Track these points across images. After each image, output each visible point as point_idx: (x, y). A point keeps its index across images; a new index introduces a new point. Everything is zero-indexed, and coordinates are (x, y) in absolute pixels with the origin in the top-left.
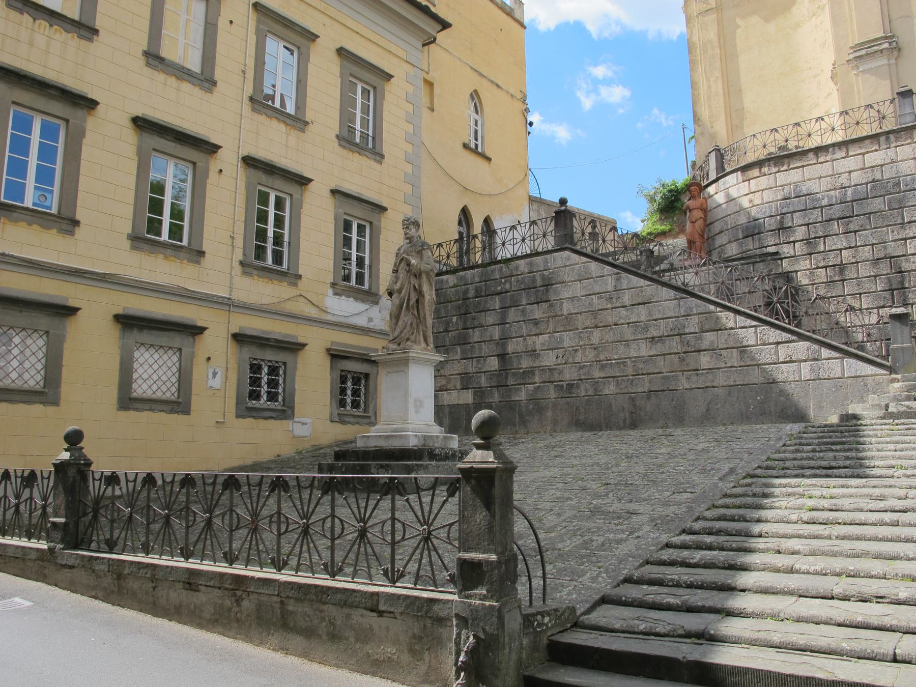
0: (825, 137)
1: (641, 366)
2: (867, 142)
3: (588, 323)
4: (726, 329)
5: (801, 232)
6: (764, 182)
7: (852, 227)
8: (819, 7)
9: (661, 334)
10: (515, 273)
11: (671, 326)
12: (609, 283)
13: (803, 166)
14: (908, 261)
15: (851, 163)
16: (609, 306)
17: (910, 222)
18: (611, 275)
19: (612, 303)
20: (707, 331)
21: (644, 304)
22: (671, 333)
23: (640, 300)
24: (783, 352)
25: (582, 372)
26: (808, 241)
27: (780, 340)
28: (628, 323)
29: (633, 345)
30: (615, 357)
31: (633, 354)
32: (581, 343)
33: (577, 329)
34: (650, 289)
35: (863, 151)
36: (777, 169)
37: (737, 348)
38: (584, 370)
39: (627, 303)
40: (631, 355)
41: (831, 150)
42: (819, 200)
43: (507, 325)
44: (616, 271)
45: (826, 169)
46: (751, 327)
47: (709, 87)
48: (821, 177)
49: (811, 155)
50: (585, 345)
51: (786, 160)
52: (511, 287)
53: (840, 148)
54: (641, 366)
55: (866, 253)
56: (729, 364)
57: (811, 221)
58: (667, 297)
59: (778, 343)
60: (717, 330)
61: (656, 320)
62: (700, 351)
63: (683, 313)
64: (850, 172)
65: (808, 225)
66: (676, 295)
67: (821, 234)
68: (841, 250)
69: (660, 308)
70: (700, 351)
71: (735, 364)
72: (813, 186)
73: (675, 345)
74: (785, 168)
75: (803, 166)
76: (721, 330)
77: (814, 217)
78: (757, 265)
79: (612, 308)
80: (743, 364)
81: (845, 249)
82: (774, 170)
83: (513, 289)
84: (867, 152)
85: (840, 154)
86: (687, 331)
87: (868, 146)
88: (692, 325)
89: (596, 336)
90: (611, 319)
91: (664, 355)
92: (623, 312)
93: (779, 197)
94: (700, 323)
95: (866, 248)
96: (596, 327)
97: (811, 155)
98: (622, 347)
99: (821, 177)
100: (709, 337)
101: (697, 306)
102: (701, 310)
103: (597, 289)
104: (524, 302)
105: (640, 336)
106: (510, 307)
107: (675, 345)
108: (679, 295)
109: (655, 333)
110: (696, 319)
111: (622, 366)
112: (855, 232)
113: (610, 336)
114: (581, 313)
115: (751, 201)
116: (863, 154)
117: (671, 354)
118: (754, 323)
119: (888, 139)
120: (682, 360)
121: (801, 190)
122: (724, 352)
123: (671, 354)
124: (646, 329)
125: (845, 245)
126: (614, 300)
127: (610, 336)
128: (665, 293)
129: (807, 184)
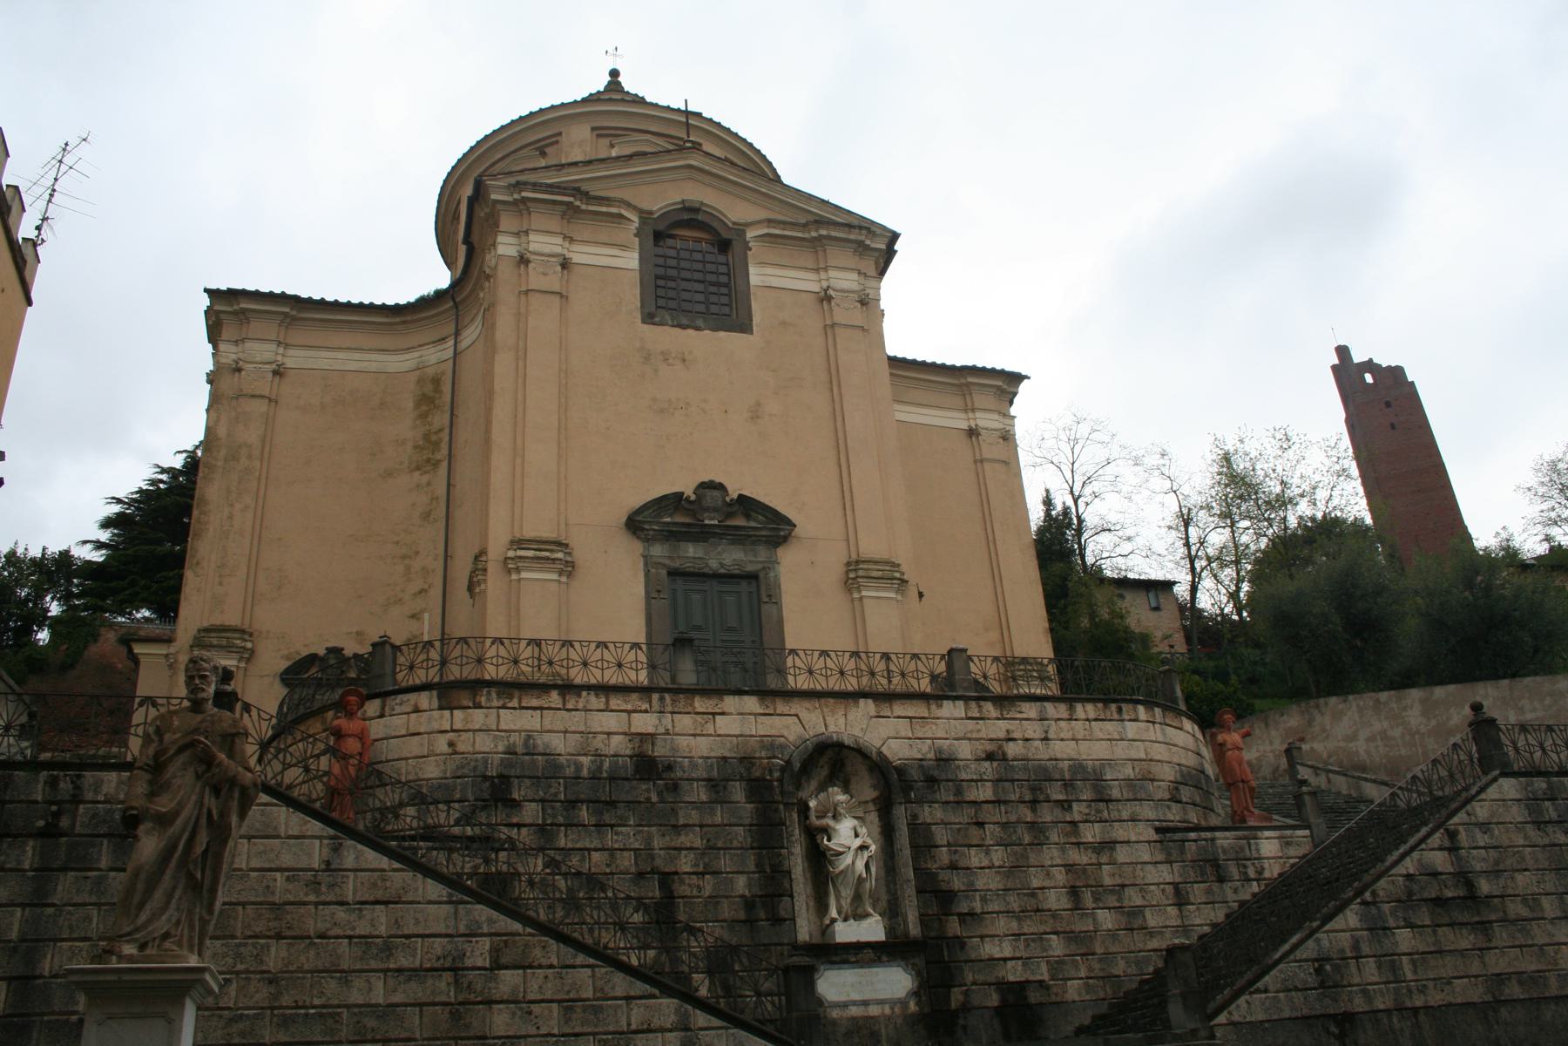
0: (607, 674)
1: (371, 1023)
2: (635, 696)
3: (259, 928)
4: (540, 967)
5: (531, 812)
6: (478, 717)
7: (607, 818)
8: (428, 460)
9: (417, 964)
10: (89, 796)
11: (439, 951)
12: (315, 854)
13: (541, 708)
14: (682, 882)
15: (611, 721)
16: (312, 898)
17: (686, 826)
18: (320, 838)
19: (317, 892)
20: (506, 968)
21: (386, 903)
22: (438, 965)
23: (379, 895)
24: (636, 1015)
25: (235, 1028)
26: (542, 830)
27: (632, 993)
28: (350, 937)
29: (358, 982)
30: (317, 1002)
31: (356, 997)
32: (240, 967)
33: (233, 937)
34: (401, 878)
35: (629, 707)
36: (501, 703)
37: (559, 1001)
38: (241, 1025)
39: (350, 898)
40: (352, 1000)
41: (584, 693)
42: (561, 767)
43: (50, 910)
44: (332, 832)
45: (575, 721)
46: (583, 966)
47: (231, 517)
48: (566, 732)
49: (555, 695)
50: (247, 971)
51: (517, 693)
52: (73, 825)
53: (597, 695)
54: (371, 1023)
55: (627, 861)
56: (543, 1031)
57: (547, 797)
58: (434, 897)
59: (628, 998)
60: (524, 968)
61: (408, 937)
62: (490, 1002)
63: (462, 929)
64: (609, 734)
65: (542, 801)
66: (450, 895)
67: (561, 820)
68: (589, 850)
69: (418, 915)
70: (490, 1002)
71: (556, 1031)
72: (558, 744)
73: (443, 987)
74: (515, 703)
75: (541, 708)
76: (531, 967)
77: (553, 790)
78: (455, 856)
79: (317, 904)
80: (567, 1030)
81: (596, 850)
82: (495, 703)
83: (78, 829)
84: (635, 711)
85: (595, 701)
86: (468, 963)
87: (634, 701)
88: (479, 953)
89: (276, 956)
90: (311, 926)
91: (421, 1005)
92: (341, 914)
93: (500, 749)
94: (495, 952)
95: (626, 854)
96: (279, 936)
97: (555, 695)
98: (333, 984)
99: (566, 732)
100: (509, 980)
101: (491, 921)
102: (496, 928)
103: (287, 860)
104: (103, 864)
105: (373, 964)
106: (65, 869)
107: (443, 987)
108: (458, 896)
109: (404, 961)
110: (485, 944)
111: (330, 1021)
112: (612, 826)
113: (308, 959)
114: (244, 904)
115: (451, 744)
116: (629, 712)
117: (434, 1004)
118: (592, 961)
119: (662, 699)
120: (456, 1016)
121: (535, 746)
122: (536, 1008)
123: (434, 1004)
124: (388, 950)
125: (596, 843)
126: (324, 889)
127: (308, 959)
128: (434, 889)
129: (546, 737)
